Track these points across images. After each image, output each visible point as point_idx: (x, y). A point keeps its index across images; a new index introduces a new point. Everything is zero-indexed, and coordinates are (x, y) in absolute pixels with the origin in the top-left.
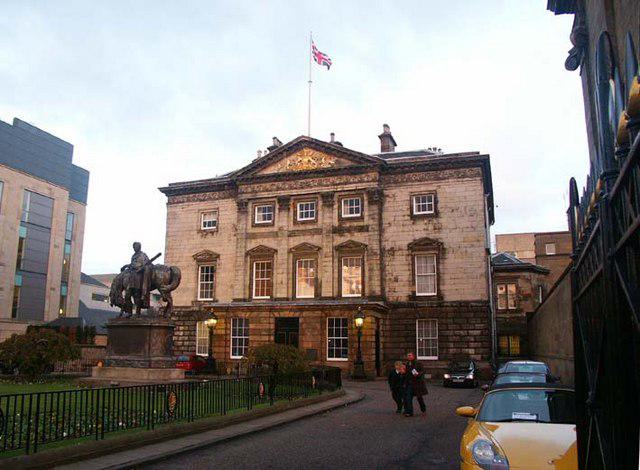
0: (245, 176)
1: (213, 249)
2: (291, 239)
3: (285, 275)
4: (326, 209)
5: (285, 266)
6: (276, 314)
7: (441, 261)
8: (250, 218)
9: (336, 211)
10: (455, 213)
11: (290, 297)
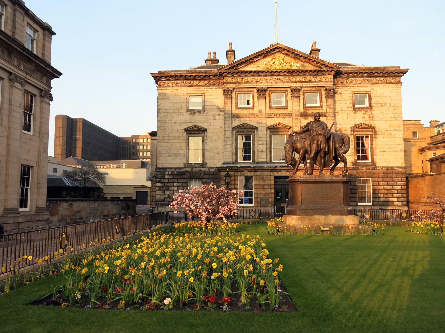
0: (233, 70)
1: (201, 125)
2: (268, 119)
3: (265, 146)
4: (295, 100)
5: (265, 139)
6: (276, 174)
7: (374, 139)
8: (234, 102)
9: (302, 102)
10: (383, 108)
11: (269, 161)
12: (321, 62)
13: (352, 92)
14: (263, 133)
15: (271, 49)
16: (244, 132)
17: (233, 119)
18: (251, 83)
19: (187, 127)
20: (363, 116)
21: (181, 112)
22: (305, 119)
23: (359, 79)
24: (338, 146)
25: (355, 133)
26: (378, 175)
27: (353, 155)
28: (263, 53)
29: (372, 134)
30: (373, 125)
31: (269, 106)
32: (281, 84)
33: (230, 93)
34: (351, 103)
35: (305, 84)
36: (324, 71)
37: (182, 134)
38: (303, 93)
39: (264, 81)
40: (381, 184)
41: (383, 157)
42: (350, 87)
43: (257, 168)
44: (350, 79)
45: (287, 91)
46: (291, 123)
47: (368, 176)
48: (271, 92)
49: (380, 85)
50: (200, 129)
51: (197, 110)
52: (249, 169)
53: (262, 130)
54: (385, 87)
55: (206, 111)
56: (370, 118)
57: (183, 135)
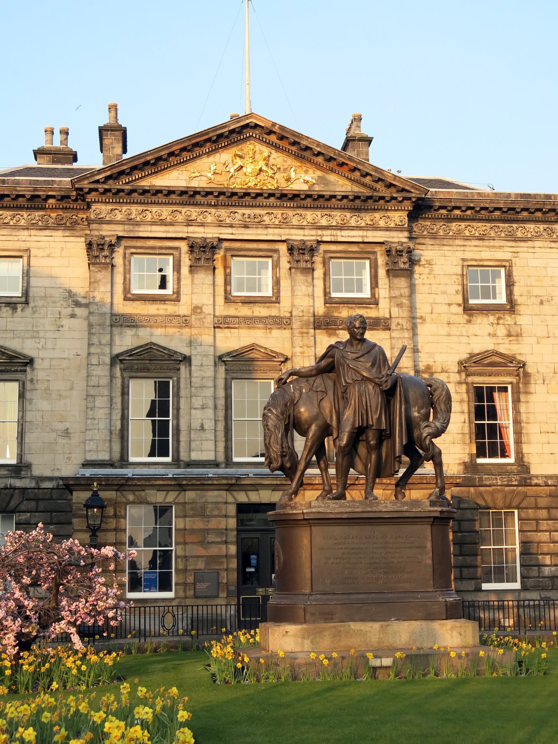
2: (220, 334)
3: (210, 413)
4: (300, 277)
5: (209, 392)
6: (242, 497)
7: (523, 398)
8: (119, 279)
9: (319, 284)
10: (546, 308)
11: (221, 458)
12: (373, 173)
13: (461, 262)
14: (204, 375)
15: (232, 127)
16: (148, 370)
17: (116, 331)
18: (171, 224)
20: (491, 329)
22: (330, 335)
23: (480, 224)
24: (416, 414)
25: (470, 379)
26: (536, 500)
27: (464, 443)
28: (209, 140)
29: (518, 383)
30: (519, 357)
31: (223, 293)
32: (260, 231)
33: (106, 253)
34: (457, 292)
35: (329, 232)
36: (382, 198)
38: (324, 258)
39: (209, 219)
40: (544, 525)
41: (547, 449)
42: (455, 248)
43: (185, 479)
44: (454, 226)
45: (276, 251)
46: (288, 345)
47: (507, 504)
48: (229, 254)
49: (537, 244)
50: (11, 357)
52: (161, 482)
53: (202, 365)
54: (549, 250)
56: (509, 335)
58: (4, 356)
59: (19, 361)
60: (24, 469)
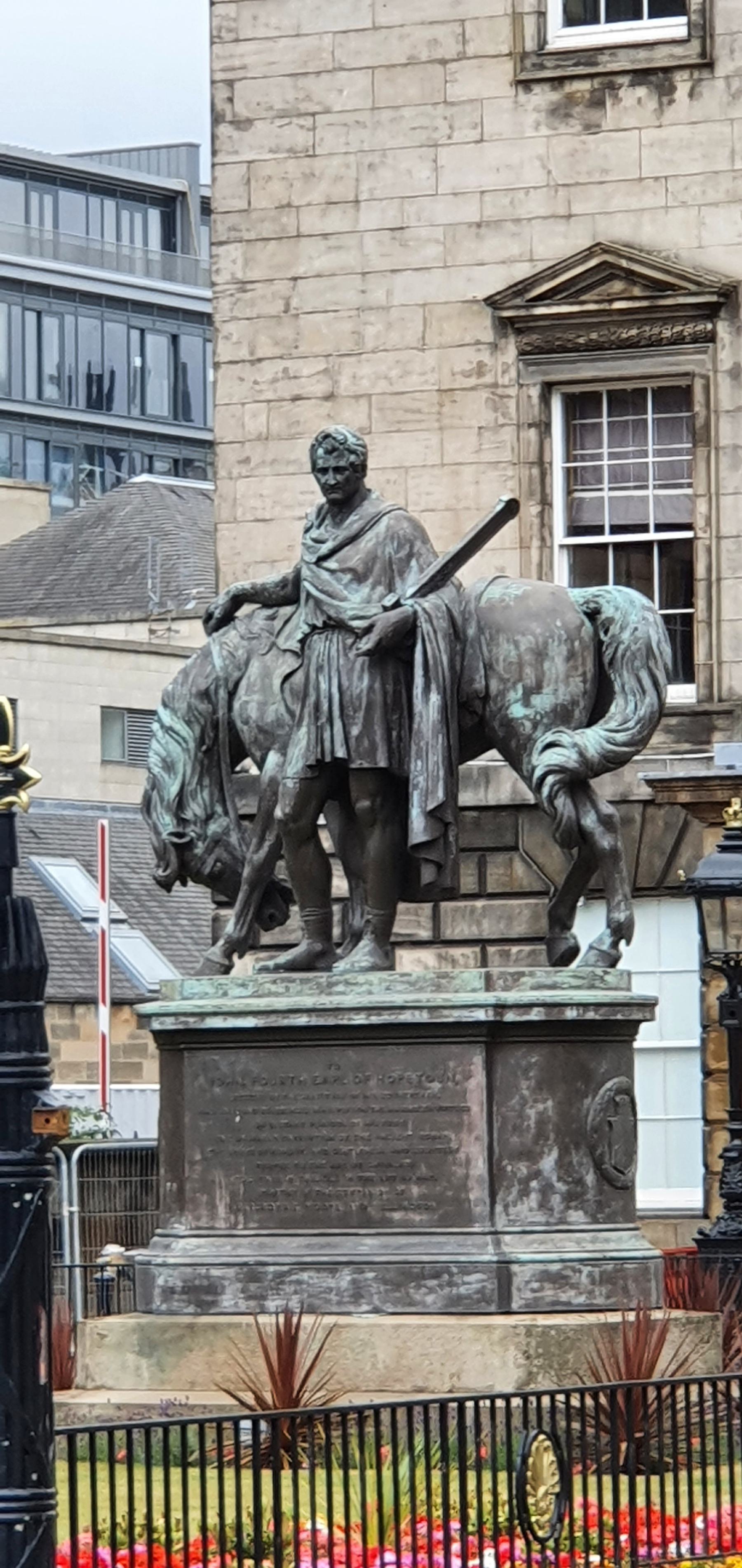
19: (522, 271)
21: (455, 92)
37: (466, 359)
51: (623, 62)
55: (723, 68)
57: (480, 369)
58: (635, 283)
59: (682, 300)
60: (720, 722)
